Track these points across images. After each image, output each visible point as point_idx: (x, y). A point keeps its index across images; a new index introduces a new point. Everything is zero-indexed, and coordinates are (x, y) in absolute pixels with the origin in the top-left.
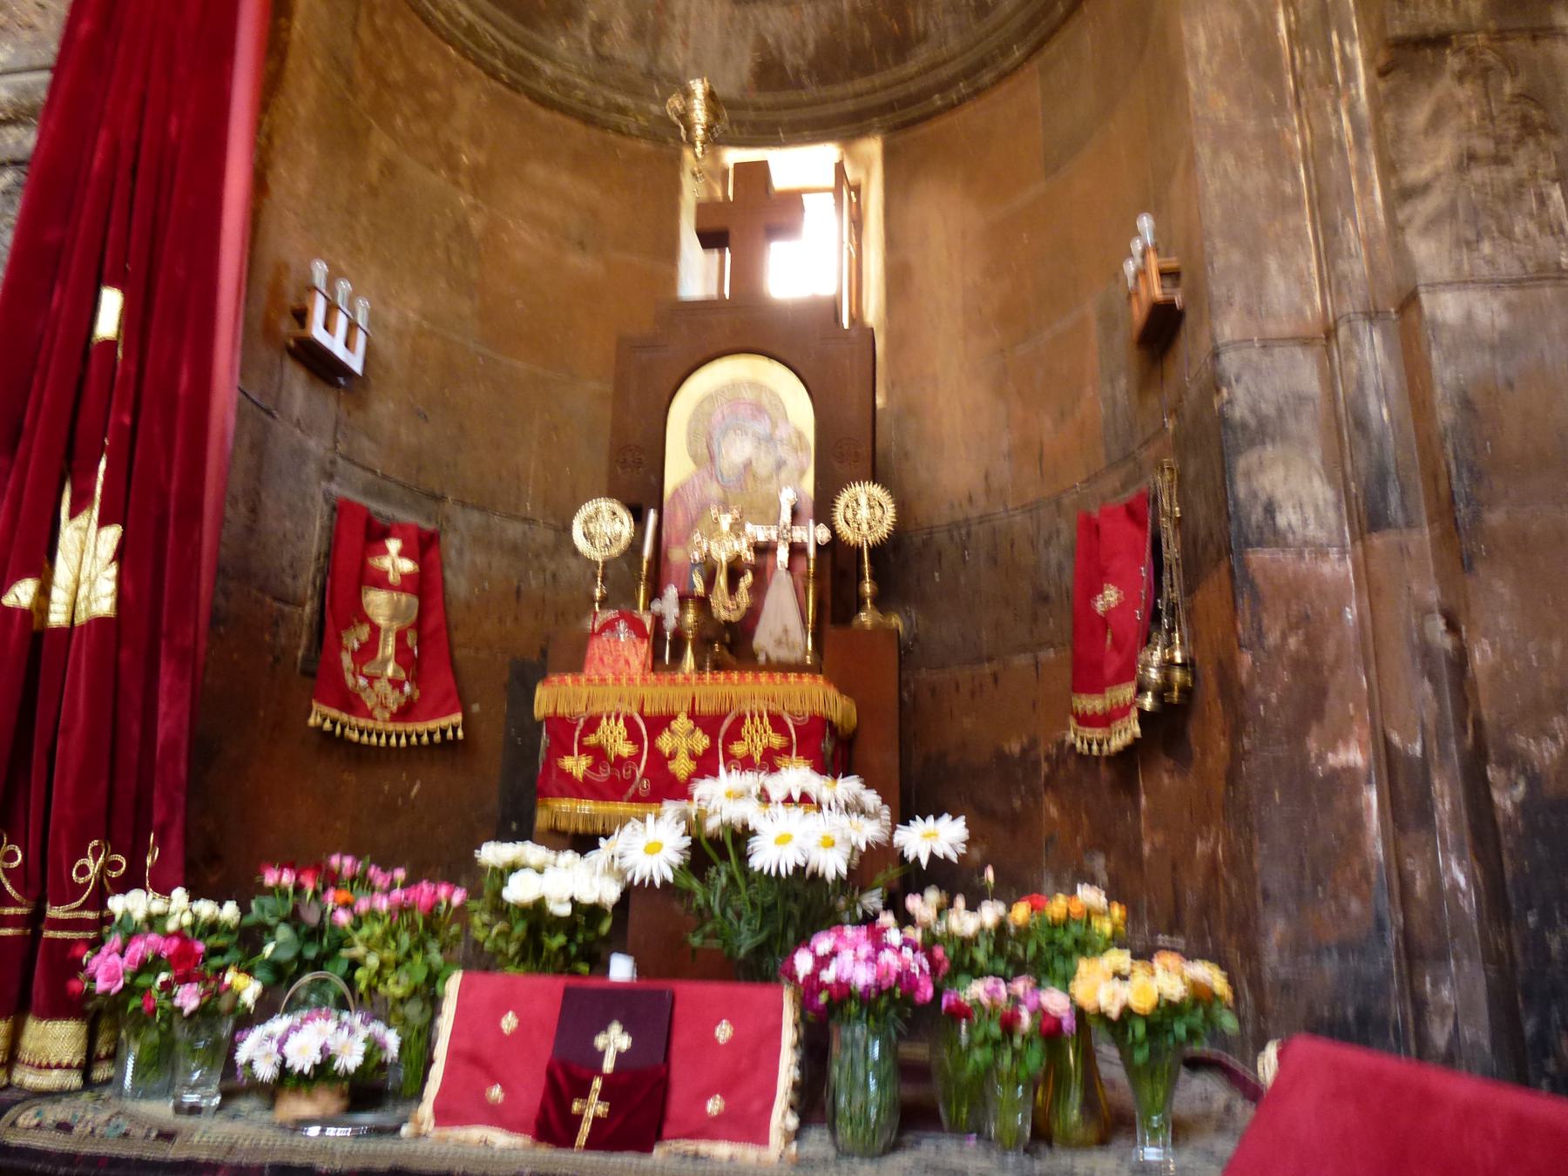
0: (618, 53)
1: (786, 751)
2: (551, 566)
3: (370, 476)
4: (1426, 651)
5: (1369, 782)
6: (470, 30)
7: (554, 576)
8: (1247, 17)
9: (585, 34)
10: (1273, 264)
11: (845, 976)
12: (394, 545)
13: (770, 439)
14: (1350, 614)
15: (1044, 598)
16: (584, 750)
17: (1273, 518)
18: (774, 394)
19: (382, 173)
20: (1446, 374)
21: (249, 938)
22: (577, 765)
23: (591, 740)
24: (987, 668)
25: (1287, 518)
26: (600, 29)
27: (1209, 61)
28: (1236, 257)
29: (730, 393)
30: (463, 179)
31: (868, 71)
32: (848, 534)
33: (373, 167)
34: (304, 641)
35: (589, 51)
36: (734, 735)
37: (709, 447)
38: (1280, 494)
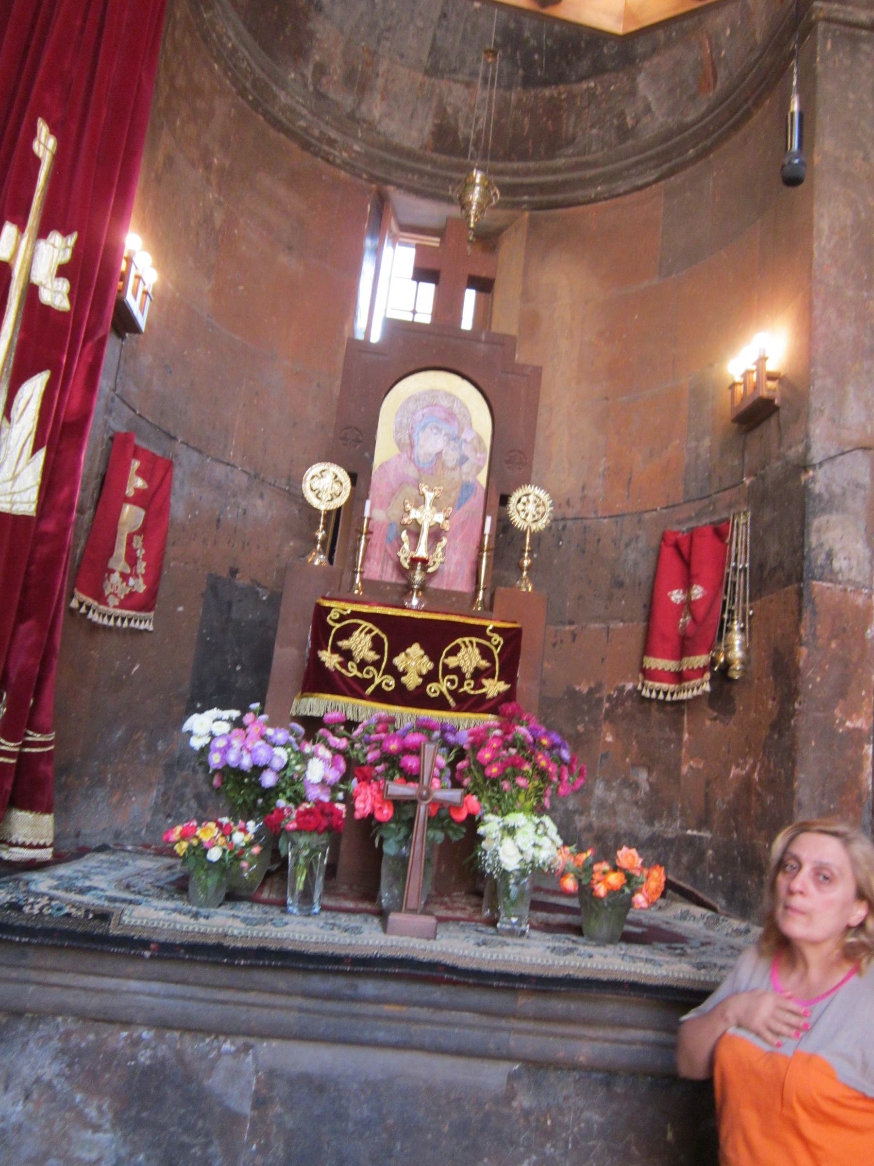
0: (331, 95)
1: (489, 673)
2: (244, 504)
3: (132, 413)
5: (869, 743)
8: (857, 213)
9: (309, 72)
10: (851, 390)
13: (456, 438)
15: (620, 585)
17: (831, 563)
18: (463, 406)
19: (164, 164)
24: (567, 628)
25: (839, 563)
26: (321, 70)
27: (829, 240)
28: (829, 382)
29: (431, 399)
30: (213, 178)
31: (524, 156)
33: (161, 158)
34: (82, 542)
35: (311, 88)
37: (410, 437)
38: (837, 547)
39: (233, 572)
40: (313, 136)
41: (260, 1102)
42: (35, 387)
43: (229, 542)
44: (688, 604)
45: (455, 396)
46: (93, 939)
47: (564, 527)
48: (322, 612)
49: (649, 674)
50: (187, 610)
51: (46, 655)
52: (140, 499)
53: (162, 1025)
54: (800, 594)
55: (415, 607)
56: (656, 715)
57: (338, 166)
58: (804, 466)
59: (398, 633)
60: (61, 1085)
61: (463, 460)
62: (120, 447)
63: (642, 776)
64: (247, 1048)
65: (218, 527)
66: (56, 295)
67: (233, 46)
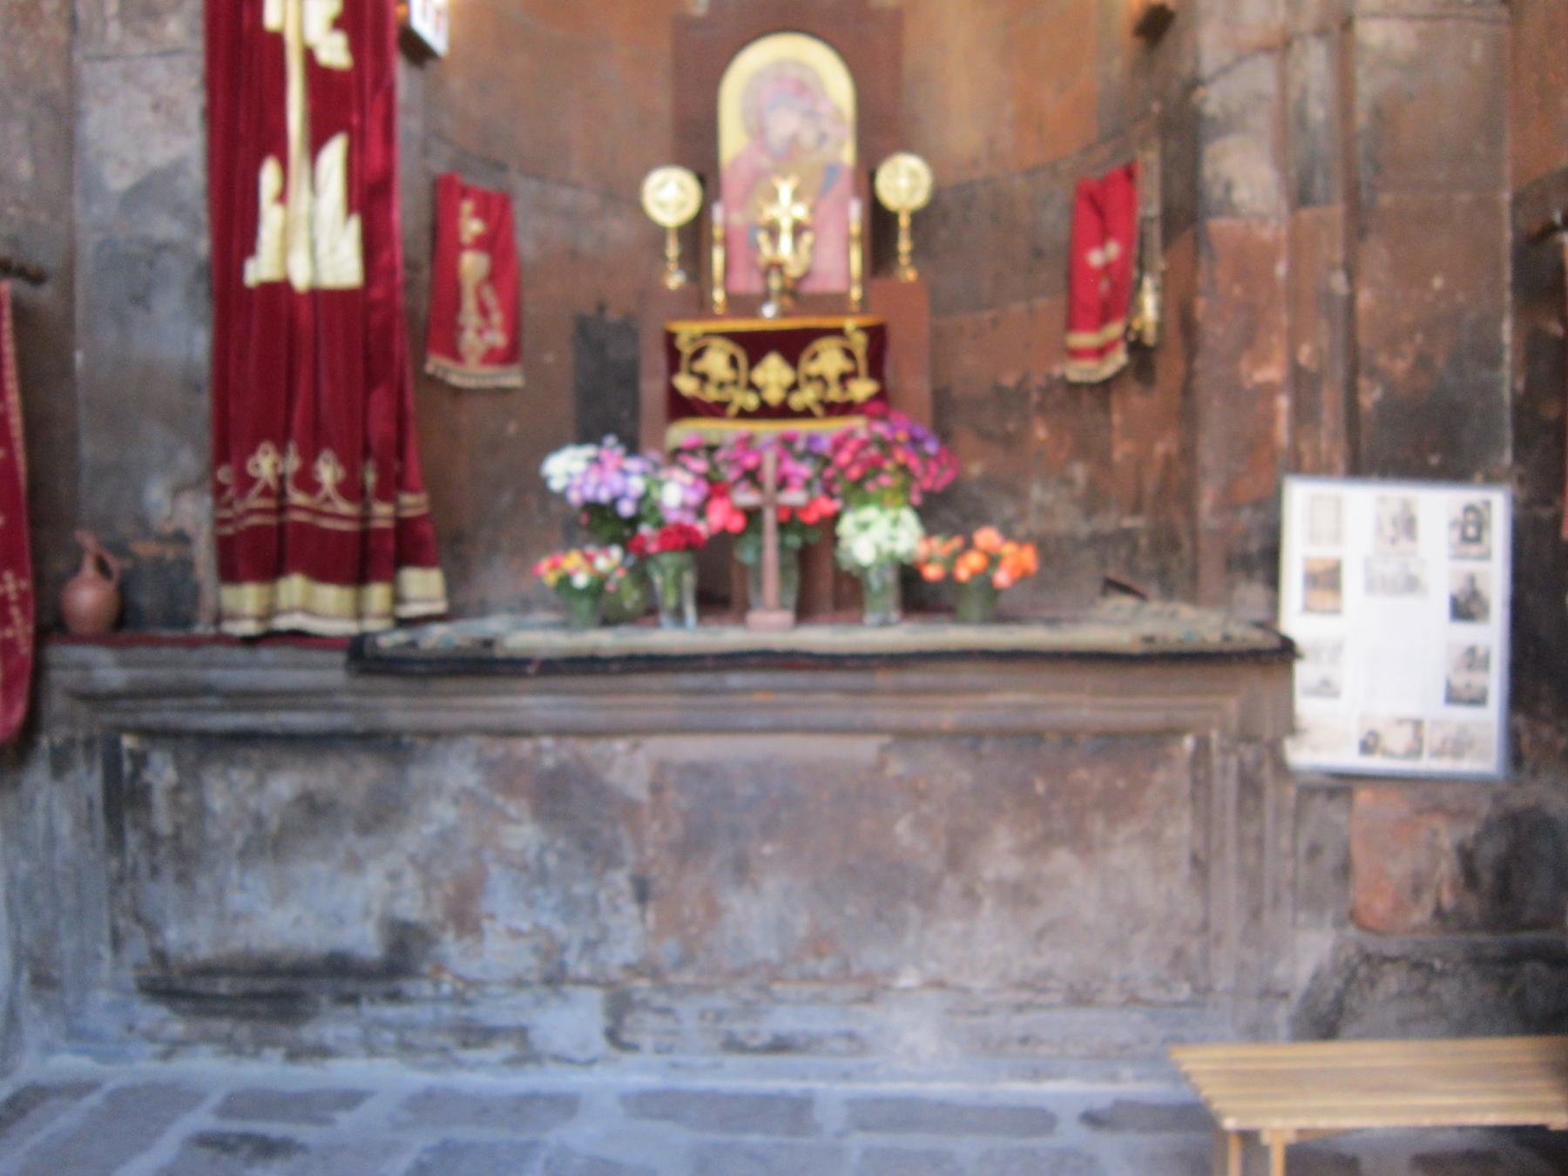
4: (1329, 295)
14: (1281, 270)
15: (1038, 253)
20: (1367, 88)
24: (988, 315)
25: (1241, 194)
39: (601, 308)
41: (656, 789)
42: (335, 153)
44: (1108, 268)
46: (483, 665)
48: (671, 337)
49: (1076, 354)
50: (557, 357)
51: (401, 420)
52: (482, 244)
53: (560, 732)
54: (1196, 238)
55: (769, 316)
56: (1087, 399)
58: (1195, 83)
59: (755, 346)
60: (484, 791)
61: (822, 138)
62: (445, 195)
63: (1079, 472)
64: (636, 747)
66: (335, 52)
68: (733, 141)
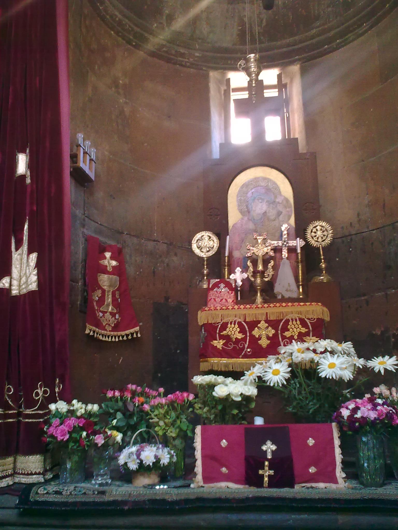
1: (307, 334)
6: (120, 23)
7: (168, 265)
11: (365, 416)
12: (108, 255)
15: (389, 267)
16: (222, 337)
18: (275, 183)
21: (105, 417)
22: (219, 344)
23: (224, 333)
30: (121, 91)
32: (313, 242)
36: (285, 329)
39: (167, 299)
40: (172, 55)
43: (162, 283)
45: (269, 179)
47: (351, 239)
57: (189, 67)
65: (154, 276)
67: (119, 19)
68: (234, 216)
